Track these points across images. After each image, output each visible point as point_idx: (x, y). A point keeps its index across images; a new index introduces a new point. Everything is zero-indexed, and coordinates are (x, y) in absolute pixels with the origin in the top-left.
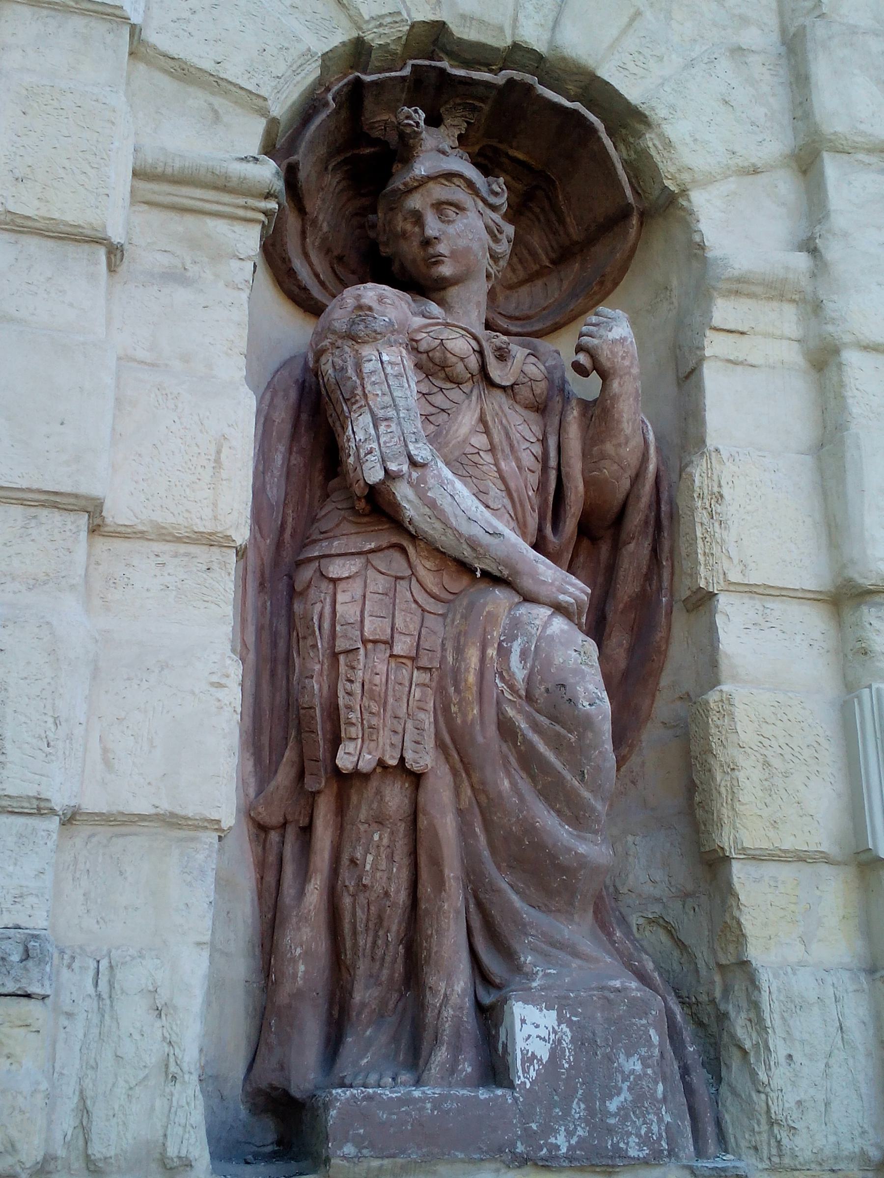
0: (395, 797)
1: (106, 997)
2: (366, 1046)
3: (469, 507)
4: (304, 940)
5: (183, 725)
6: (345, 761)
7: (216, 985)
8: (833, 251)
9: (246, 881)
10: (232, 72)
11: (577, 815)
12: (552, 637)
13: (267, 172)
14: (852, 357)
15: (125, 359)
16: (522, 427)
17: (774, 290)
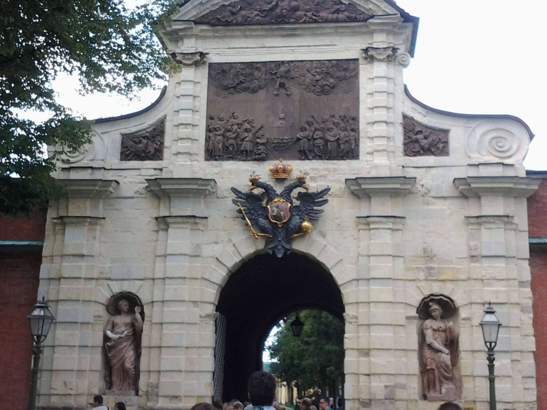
9: (421, 378)
10: (414, 304)
12: (446, 358)
13: (417, 315)
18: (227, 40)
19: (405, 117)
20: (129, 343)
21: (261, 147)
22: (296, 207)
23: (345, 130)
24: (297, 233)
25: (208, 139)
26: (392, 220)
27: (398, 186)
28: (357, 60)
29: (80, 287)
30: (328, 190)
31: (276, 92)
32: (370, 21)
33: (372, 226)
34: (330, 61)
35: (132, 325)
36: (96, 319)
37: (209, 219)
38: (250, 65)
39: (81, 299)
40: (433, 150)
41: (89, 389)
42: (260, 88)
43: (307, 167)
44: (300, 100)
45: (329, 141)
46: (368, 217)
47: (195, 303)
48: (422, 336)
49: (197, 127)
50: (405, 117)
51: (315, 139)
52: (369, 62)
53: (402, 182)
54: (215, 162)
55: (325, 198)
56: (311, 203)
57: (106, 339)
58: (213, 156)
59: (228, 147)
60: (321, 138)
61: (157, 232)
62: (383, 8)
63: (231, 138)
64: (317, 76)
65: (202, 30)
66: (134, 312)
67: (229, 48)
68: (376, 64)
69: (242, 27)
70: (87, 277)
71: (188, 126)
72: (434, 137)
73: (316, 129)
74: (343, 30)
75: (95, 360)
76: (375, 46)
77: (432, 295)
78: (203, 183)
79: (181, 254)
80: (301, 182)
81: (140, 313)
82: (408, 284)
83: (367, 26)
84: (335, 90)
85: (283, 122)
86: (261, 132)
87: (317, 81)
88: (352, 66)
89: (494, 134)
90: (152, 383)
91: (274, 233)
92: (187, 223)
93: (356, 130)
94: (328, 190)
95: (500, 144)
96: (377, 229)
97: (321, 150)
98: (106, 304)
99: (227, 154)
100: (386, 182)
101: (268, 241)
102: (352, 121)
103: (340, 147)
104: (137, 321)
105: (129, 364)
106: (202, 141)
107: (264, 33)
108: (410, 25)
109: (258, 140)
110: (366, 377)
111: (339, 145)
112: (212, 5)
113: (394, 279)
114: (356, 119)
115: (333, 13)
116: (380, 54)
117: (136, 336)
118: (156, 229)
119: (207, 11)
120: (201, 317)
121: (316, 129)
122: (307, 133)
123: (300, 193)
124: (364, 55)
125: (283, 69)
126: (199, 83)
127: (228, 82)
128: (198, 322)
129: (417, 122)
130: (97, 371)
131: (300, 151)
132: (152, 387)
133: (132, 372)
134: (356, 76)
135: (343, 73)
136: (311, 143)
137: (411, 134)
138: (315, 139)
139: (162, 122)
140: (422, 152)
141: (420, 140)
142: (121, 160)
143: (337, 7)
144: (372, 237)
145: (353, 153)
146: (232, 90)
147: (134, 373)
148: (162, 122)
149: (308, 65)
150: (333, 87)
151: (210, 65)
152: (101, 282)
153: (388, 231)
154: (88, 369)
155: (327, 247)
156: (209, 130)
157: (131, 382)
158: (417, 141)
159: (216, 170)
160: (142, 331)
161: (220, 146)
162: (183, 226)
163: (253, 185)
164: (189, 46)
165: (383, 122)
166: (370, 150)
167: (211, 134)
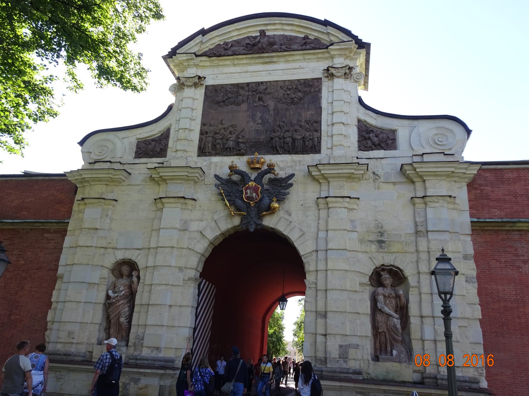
0: (383, 334)
1: (363, 349)
2: (383, 352)
3: (387, 310)
4: (378, 344)
5: (367, 329)
6: (379, 331)
7: (371, 348)
8: (421, 284)
9: (373, 340)
10: (366, 273)
11: (398, 336)
14: (422, 294)
15: (360, 300)
16: (394, 301)
17: (416, 287)
18: (221, 69)
19: (359, 121)
20: (126, 301)
21: (241, 145)
22: (267, 190)
23: (310, 130)
24: (266, 211)
25: (201, 140)
26: (348, 199)
27: (353, 171)
28: (321, 78)
30: (293, 175)
31: (256, 104)
32: (330, 47)
33: (330, 206)
34: (299, 80)
35: (130, 287)
37: (197, 202)
38: (238, 86)
39: (90, 263)
40: (383, 145)
42: (243, 101)
43: (278, 160)
44: (274, 110)
45: (295, 139)
46: (326, 197)
47: (180, 269)
48: (374, 300)
49: (193, 132)
50: (359, 121)
51: (284, 138)
52: (329, 80)
53: (355, 167)
54: (205, 158)
55: (290, 182)
56: (280, 187)
57: (108, 297)
58: (203, 153)
59: (215, 145)
60: (289, 137)
61: (156, 211)
62: (341, 38)
63: (218, 139)
64: (288, 92)
65: (201, 61)
66: (132, 276)
67: (221, 74)
68: (336, 80)
69: (232, 57)
71: (186, 130)
72: (385, 136)
73: (286, 131)
74: (310, 57)
75: (96, 315)
76: (334, 66)
77: (383, 265)
78: (192, 171)
79: (171, 228)
80: (271, 168)
81: (136, 276)
82: (361, 255)
83: (328, 52)
84: (302, 101)
85: (260, 126)
86: (242, 134)
87: (288, 94)
88: (316, 84)
89: (435, 132)
90: (139, 336)
91: (248, 211)
92: (179, 203)
93: (318, 130)
94: (293, 175)
95: (440, 139)
96: (335, 207)
97: (289, 146)
99: (216, 151)
100: (341, 167)
101: (243, 218)
102: (315, 124)
103: (305, 144)
106: (197, 142)
107: (248, 61)
108: (363, 52)
109: (240, 140)
110: (322, 337)
111: (304, 142)
112: (211, 45)
113: (349, 251)
114: (319, 122)
115: (302, 46)
116: (338, 72)
117: (131, 295)
118: (156, 209)
119: (207, 49)
120: (184, 280)
121: (286, 131)
122: (278, 134)
123: (270, 178)
124: (326, 74)
125: (262, 87)
126: (197, 99)
127: (220, 98)
128: (181, 284)
129: (368, 124)
131: (272, 148)
132: (138, 339)
134: (320, 91)
135: (309, 89)
136: (282, 141)
137: (364, 134)
138: (284, 138)
139: (168, 130)
140: (373, 147)
141: (372, 138)
142: (135, 158)
143: (305, 41)
144: (330, 215)
145: (315, 148)
146: (222, 104)
148: (168, 130)
149: (282, 84)
150: (300, 100)
151: (207, 86)
152: (109, 251)
153: (344, 209)
155: (292, 223)
156: (202, 133)
157: (124, 334)
158: (369, 138)
159: (205, 163)
161: (210, 145)
162: (174, 205)
163: (231, 171)
164: (192, 72)
165: (340, 123)
166: (329, 146)
167: (203, 137)
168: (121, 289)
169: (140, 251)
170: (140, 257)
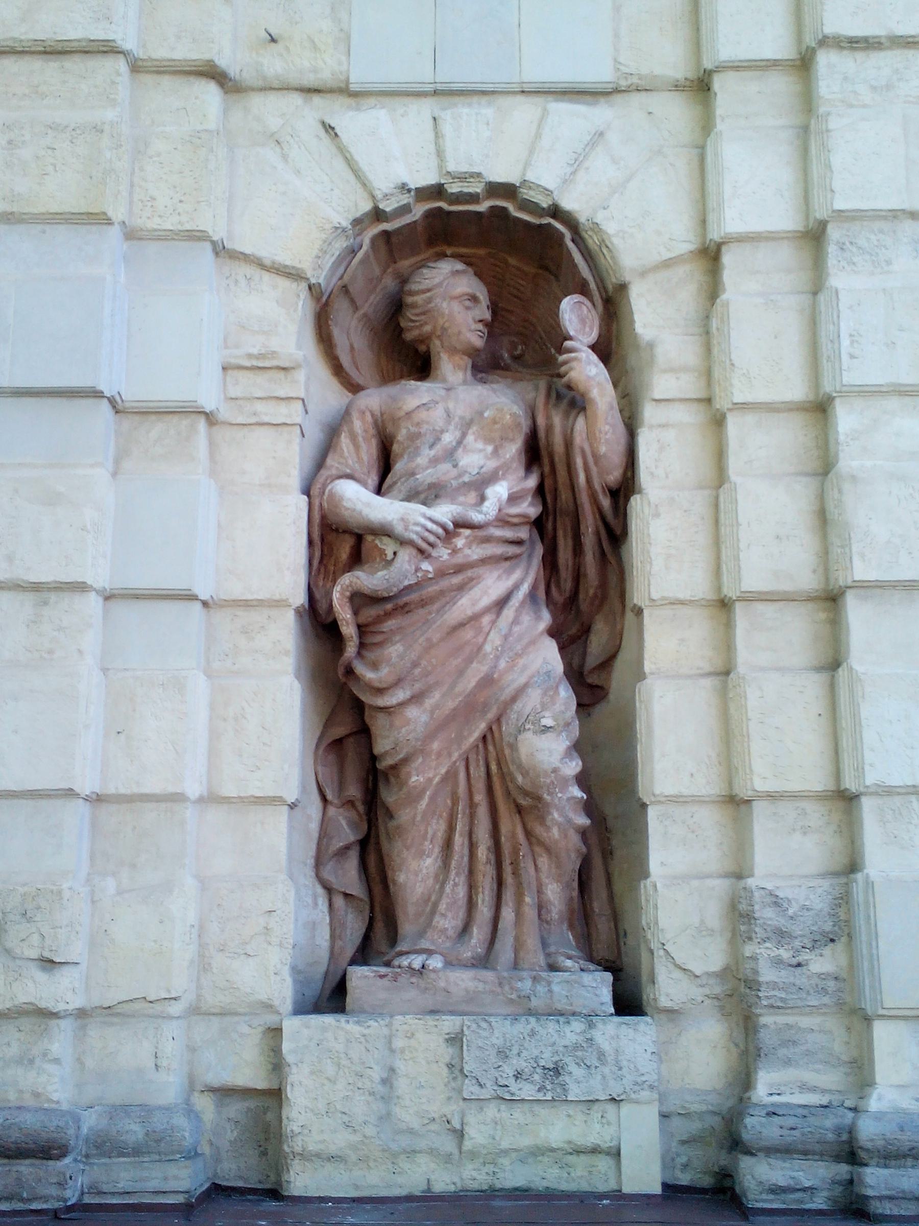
29: (110, 115)
35: (534, 452)
36: (244, 384)
39: (118, 213)
41: (203, 965)
57: (337, 543)
70: (160, 52)
81: (593, 347)
90: (777, 902)
98: (319, 277)
104: (574, 402)
105: (548, 749)
130: (274, 801)
133: (566, 812)
147: (583, 820)
152: (271, 110)
154: (193, 789)
157: (556, 894)
160: (624, 490)
168: (475, 458)
169: (599, 114)
170: (602, 168)
